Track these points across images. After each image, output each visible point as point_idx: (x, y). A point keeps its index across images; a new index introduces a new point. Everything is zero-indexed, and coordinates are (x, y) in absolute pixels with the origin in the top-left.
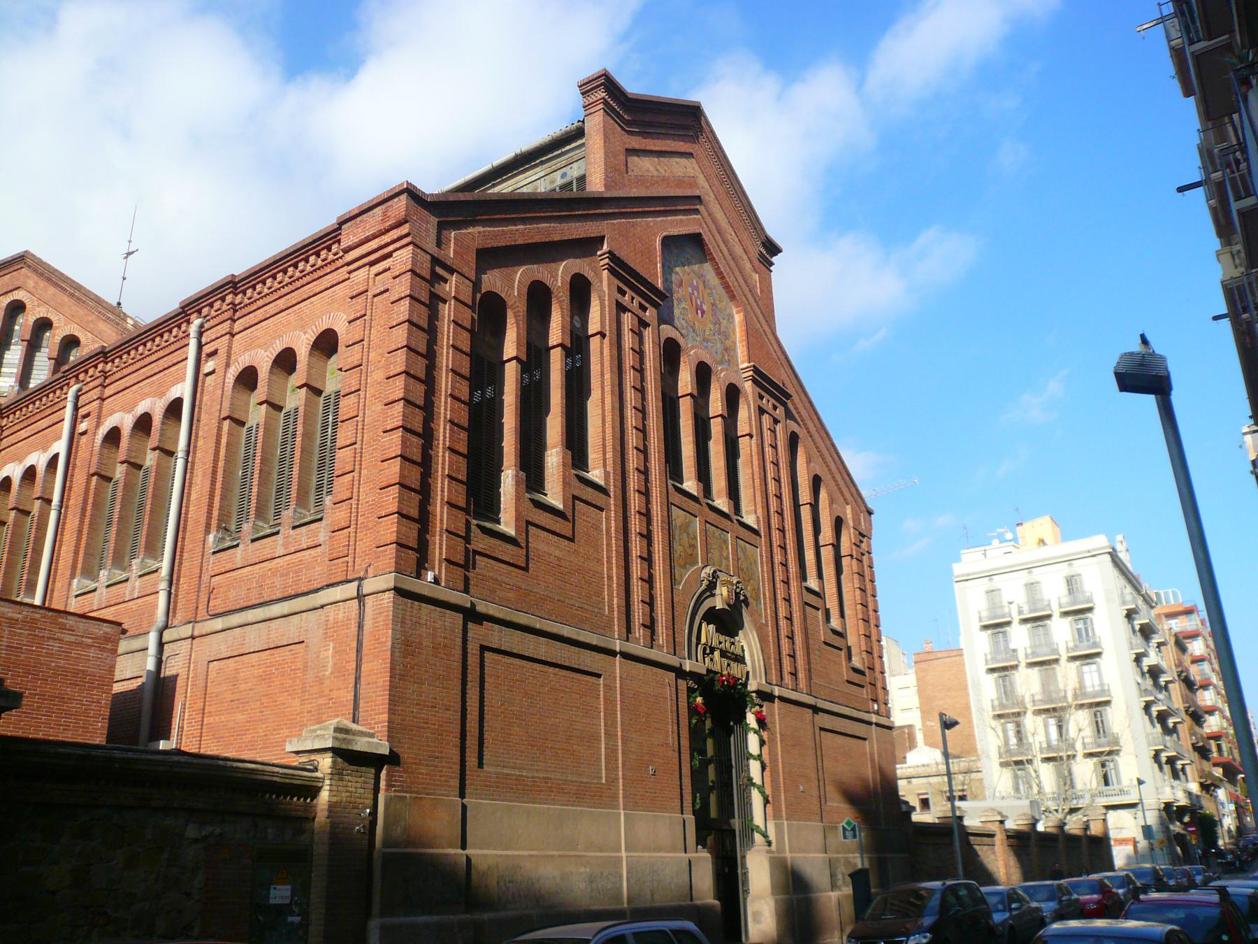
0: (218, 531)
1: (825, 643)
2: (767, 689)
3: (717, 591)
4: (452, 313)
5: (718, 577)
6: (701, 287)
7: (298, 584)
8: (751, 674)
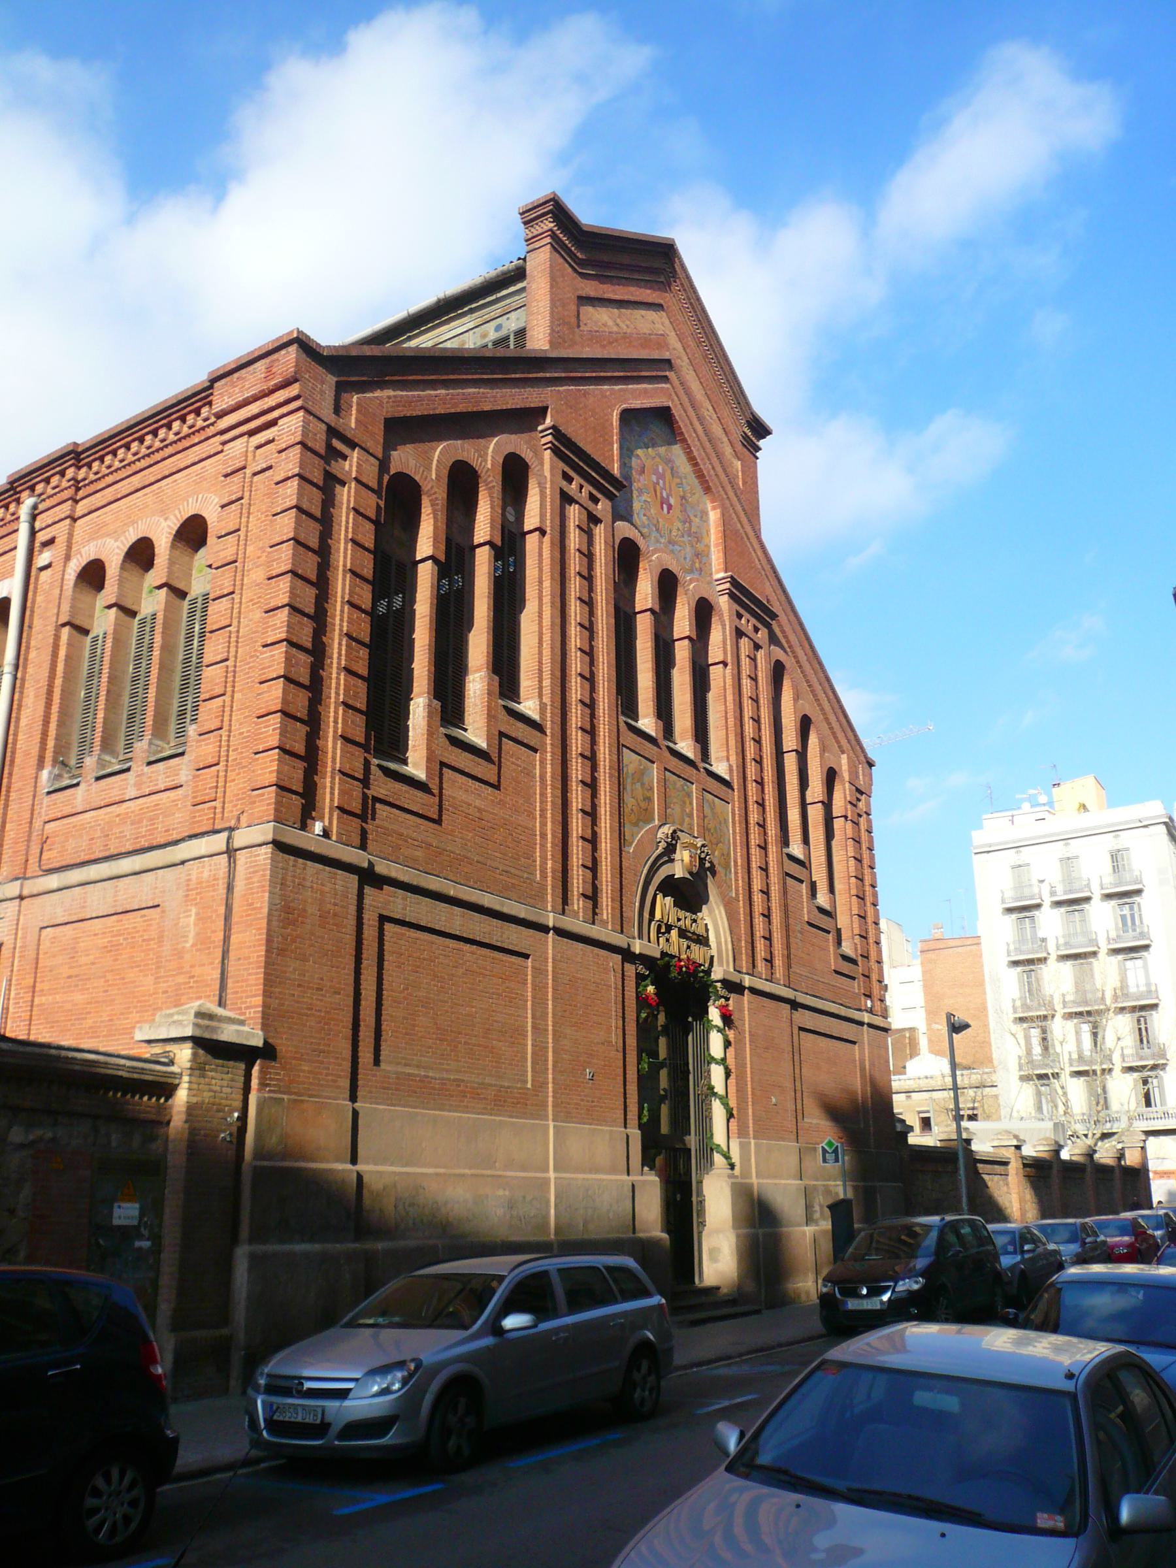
0: (53, 766)
1: (809, 924)
2: (735, 978)
3: (677, 856)
4: (352, 499)
5: (679, 838)
6: (668, 475)
7: (152, 834)
8: (715, 959)
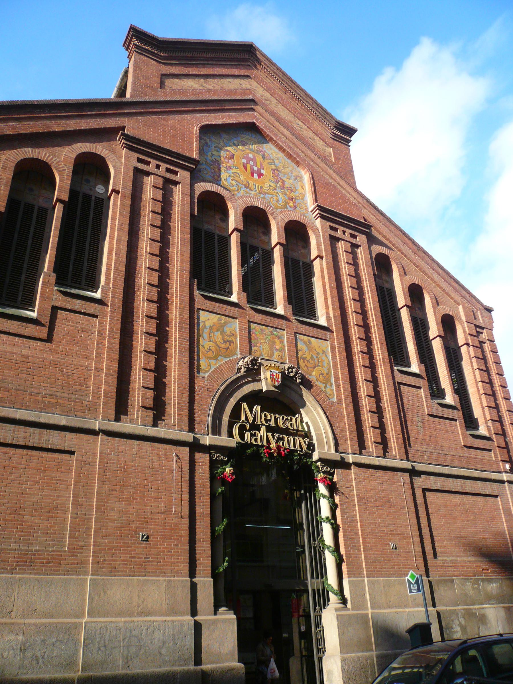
3: (262, 377)
6: (259, 158)
